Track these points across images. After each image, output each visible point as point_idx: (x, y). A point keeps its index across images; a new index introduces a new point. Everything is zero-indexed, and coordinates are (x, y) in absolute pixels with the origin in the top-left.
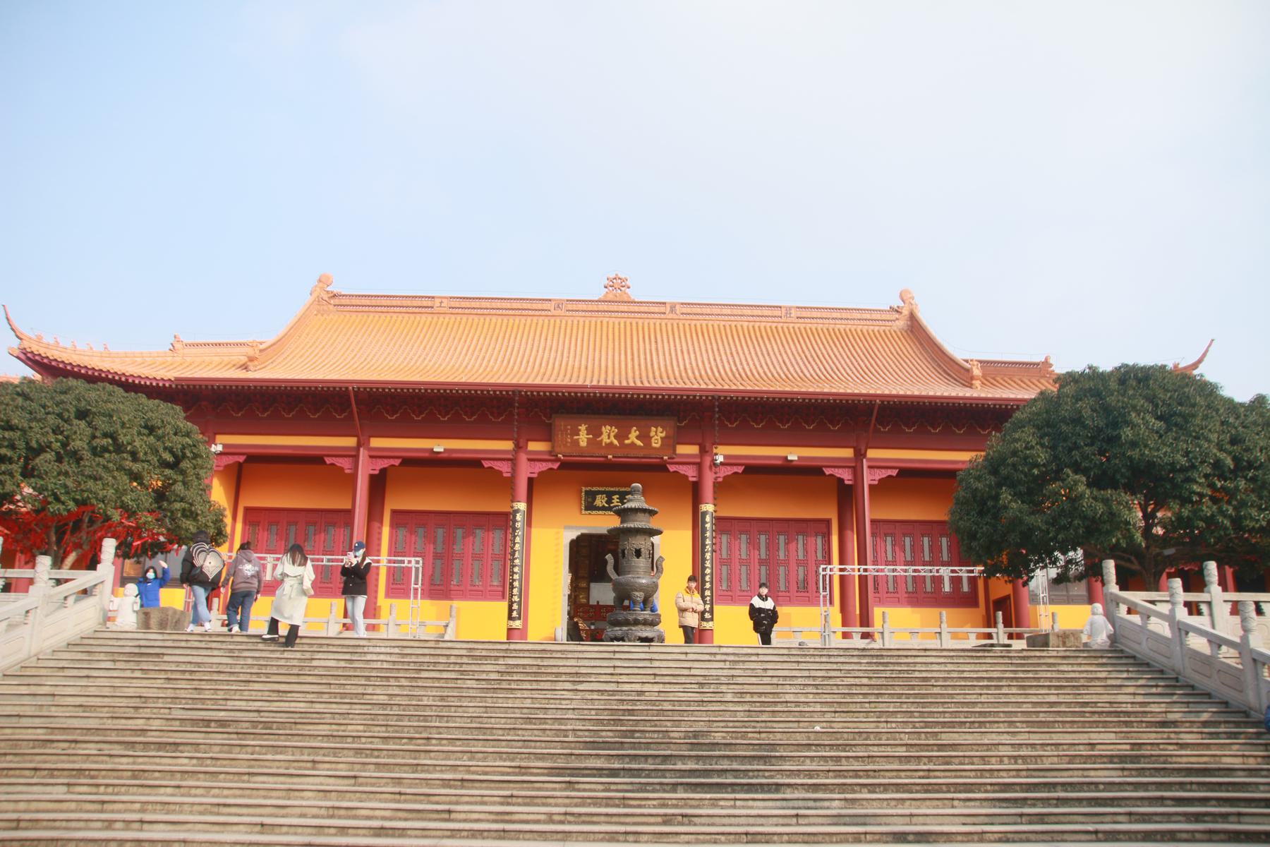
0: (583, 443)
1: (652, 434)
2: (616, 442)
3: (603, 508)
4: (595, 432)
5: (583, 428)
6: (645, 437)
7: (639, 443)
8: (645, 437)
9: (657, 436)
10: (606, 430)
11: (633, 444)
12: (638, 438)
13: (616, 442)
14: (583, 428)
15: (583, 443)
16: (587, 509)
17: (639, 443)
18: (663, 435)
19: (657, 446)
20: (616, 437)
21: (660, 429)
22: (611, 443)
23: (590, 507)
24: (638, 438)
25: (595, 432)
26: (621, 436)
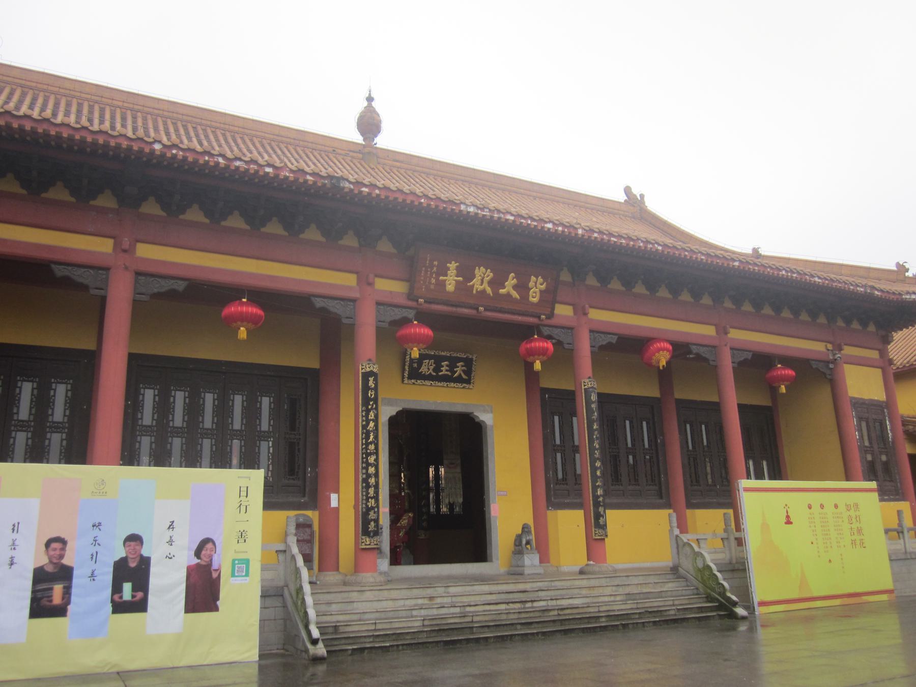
0: (450, 287)
1: (531, 284)
2: (489, 290)
3: (429, 378)
4: (466, 273)
5: (453, 266)
6: (523, 287)
7: (515, 295)
8: (523, 287)
9: (537, 287)
10: (480, 272)
11: (508, 295)
12: (515, 287)
13: (489, 290)
14: (453, 266)
15: (450, 287)
16: (410, 378)
17: (515, 295)
18: (543, 287)
19: (535, 300)
20: (490, 283)
21: (540, 280)
22: (484, 291)
23: (415, 374)
24: (515, 287)
25: (466, 273)
26: (497, 283)
